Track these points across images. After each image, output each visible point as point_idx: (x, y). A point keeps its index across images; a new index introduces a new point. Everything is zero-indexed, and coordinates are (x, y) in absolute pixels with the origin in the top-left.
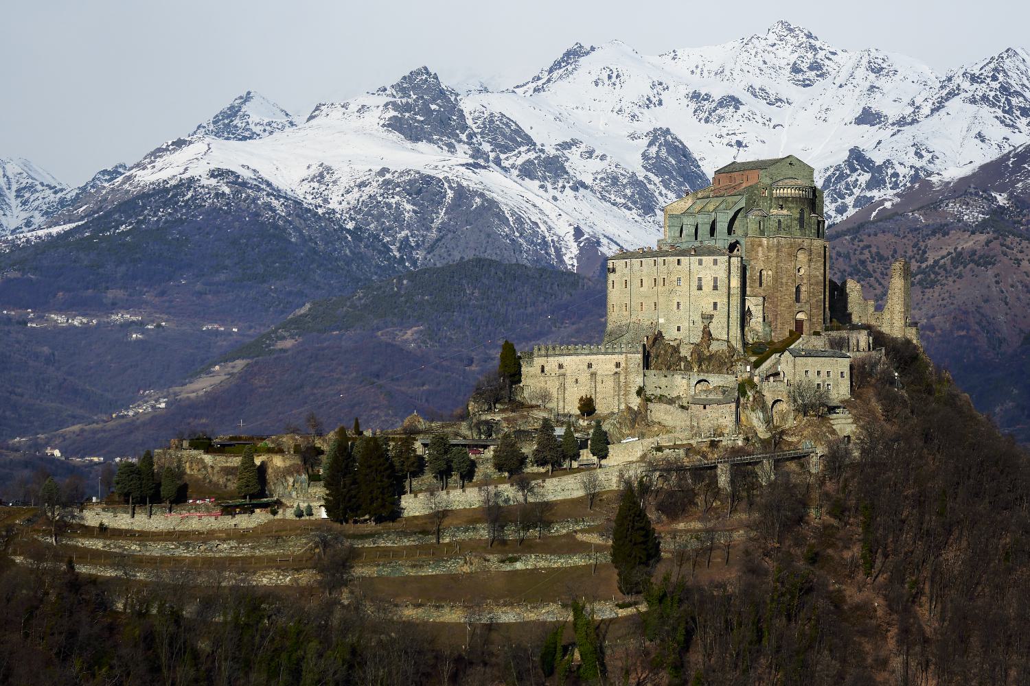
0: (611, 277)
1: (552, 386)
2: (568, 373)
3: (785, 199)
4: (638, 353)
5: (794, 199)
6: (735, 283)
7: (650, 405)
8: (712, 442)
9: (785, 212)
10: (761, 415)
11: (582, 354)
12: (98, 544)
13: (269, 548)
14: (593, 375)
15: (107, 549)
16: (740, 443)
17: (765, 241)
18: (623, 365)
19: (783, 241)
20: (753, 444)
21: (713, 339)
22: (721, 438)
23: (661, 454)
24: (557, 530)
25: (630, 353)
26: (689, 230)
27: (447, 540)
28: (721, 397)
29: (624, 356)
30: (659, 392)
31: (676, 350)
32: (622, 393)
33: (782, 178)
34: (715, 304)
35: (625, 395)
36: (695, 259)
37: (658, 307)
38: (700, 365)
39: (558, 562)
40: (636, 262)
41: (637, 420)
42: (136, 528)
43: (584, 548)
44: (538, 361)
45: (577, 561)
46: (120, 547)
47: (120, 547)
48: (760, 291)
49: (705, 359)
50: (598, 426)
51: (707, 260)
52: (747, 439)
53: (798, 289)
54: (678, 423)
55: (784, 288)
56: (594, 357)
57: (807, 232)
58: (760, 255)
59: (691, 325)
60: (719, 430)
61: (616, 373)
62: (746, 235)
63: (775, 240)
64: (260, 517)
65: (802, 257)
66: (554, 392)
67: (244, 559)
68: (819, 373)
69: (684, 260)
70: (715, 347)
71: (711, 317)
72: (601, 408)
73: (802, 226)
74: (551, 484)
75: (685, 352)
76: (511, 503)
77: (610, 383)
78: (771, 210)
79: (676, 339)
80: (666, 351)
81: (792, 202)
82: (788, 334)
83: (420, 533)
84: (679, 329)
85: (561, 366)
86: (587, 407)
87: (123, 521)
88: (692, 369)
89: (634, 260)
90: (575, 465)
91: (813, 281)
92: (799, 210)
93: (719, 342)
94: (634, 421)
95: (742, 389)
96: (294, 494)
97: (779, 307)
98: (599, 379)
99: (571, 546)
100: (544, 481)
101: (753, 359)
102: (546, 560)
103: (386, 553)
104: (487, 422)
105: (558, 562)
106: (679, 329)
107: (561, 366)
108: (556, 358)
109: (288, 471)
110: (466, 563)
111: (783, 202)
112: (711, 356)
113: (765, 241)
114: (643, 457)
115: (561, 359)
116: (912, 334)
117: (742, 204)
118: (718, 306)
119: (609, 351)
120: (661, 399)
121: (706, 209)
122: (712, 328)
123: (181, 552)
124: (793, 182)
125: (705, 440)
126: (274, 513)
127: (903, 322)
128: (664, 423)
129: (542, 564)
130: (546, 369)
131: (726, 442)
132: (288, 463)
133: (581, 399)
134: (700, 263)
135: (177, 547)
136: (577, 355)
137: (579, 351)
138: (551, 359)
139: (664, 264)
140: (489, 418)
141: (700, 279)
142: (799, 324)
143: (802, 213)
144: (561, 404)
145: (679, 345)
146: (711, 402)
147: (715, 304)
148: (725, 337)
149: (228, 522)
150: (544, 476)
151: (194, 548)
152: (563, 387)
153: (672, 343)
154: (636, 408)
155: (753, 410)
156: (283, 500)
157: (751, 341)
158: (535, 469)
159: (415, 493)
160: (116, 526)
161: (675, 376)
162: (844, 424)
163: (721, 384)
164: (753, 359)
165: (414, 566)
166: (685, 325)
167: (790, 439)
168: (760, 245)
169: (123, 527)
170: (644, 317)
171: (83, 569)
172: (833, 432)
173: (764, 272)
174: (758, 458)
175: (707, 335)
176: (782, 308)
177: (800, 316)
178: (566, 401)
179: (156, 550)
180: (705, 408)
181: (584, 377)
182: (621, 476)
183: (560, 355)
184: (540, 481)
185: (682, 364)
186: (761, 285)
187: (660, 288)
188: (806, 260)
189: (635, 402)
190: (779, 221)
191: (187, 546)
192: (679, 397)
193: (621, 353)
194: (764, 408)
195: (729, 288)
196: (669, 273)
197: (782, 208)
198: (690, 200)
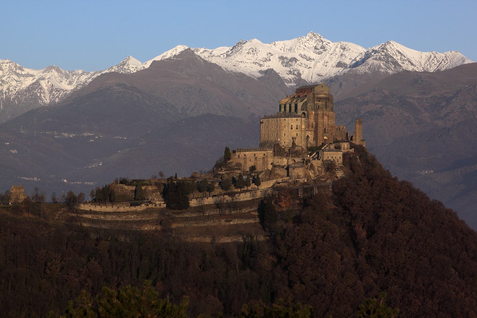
0: (262, 125)
1: (242, 162)
2: (248, 157)
6: (303, 127)
7: (275, 168)
9: (320, 103)
12: (89, 216)
13: (147, 217)
14: (256, 158)
15: (93, 218)
16: (306, 181)
19: (319, 112)
21: (296, 146)
22: (299, 179)
23: (279, 185)
24: (244, 211)
26: (288, 109)
27: (207, 214)
29: (266, 151)
31: (284, 149)
33: (319, 91)
34: (297, 134)
38: (292, 155)
39: (245, 222)
40: (270, 120)
41: (271, 174)
42: (102, 211)
43: (254, 217)
45: (252, 221)
46: (97, 217)
47: (97, 217)
48: (311, 129)
49: (293, 151)
50: (258, 176)
51: (294, 119)
52: (307, 180)
53: (325, 129)
56: (256, 152)
58: (312, 117)
61: (264, 157)
64: (143, 207)
65: (326, 118)
66: (243, 164)
67: (139, 221)
68: (332, 157)
70: (296, 149)
71: (296, 138)
72: (258, 169)
73: (326, 107)
74: (242, 195)
76: (229, 201)
77: (261, 161)
80: (280, 150)
81: (323, 99)
82: (321, 144)
83: (198, 212)
84: (285, 142)
85: (245, 155)
86: (253, 168)
87: (98, 208)
90: (250, 188)
93: (298, 147)
94: (270, 174)
96: (155, 199)
98: (258, 159)
99: (248, 216)
100: (240, 194)
101: (310, 152)
102: (241, 221)
103: (187, 219)
104: (220, 174)
105: (245, 222)
106: (285, 142)
108: (244, 153)
109: (153, 191)
110: (214, 222)
111: (320, 99)
112: (296, 151)
113: (313, 112)
115: (245, 153)
117: (306, 100)
118: (298, 134)
120: (279, 166)
123: (118, 219)
126: (148, 205)
127: (360, 139)
128: (280, 174)
129: (239, 222)
130: (240, 156)
131: (301, 181)
132: (153, 189)
135: (116, 217)
138: (241, 153)
140: (221, 173)
142: (326, 140)
143: (326, 103)
144: (245, 168)
145: (285, 148)
146: (296, 167)
147: (297, 134)
149: (133, 208)
150: (240, 193)
151: (122, 218)
152: (245, 162)
153: (283, 147)
154: (270, 169)
156: (152, 201)
157: (309, 146)
158: (236, 190)
159: (196, 198)
160: (96, 210)
162: (340, 174)
164: (310, 152)
165: (196, 223)
167: (322, 180)
168: (312, 114)
169: (98, 210)
170: (272, 139)
171: (85, 225)
172: (337, 177)
173: (313, 123)
175: (294, 144)
179: (109, 218)
180: (294, 169)
181: (253, 159)
183: (245, 151)
184: (239, 194)
185: (286, 154)
186: (312, 127)
189: (270, 167)
190: (319, 106)
191: (120, 217)
193: (265, 151)
197: (319, 101)
198: (288, 99)
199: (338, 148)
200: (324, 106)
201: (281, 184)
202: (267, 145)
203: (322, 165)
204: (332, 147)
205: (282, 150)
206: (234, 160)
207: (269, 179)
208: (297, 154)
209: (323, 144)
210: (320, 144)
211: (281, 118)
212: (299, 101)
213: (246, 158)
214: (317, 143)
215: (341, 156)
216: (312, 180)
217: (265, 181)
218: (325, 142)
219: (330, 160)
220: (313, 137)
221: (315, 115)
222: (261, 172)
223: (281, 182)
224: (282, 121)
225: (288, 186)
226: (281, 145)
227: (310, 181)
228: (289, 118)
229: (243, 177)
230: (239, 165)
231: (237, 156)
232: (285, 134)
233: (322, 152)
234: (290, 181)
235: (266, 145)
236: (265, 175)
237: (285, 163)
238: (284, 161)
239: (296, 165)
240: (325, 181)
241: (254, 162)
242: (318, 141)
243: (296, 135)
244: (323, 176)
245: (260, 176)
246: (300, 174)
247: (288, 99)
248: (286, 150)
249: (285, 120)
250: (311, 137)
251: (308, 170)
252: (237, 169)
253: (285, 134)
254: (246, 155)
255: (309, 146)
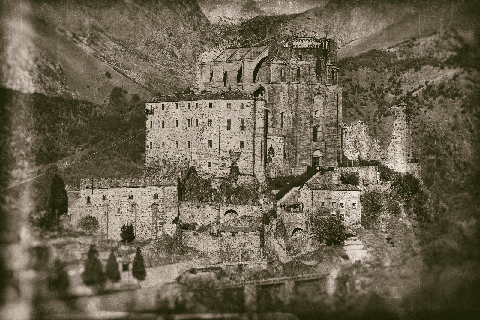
0: (150, 118)
2: (112, 203)
3: (304, 50)
4: (175, 186)
5: (312, 50)
6: (260, 124)
7: (185, 233)
8: (240, 266)
9: (303, 61)
10: (283, 242)
11: (123, 187)
14: (134, 205)
17: (286, 87)
18: (160, 197)
19: (302, 87)
20: (276, 268)
22: (247, 262)
23: (193, 276)
25: (167, 186)
28: (248, 226)
29: (161, 188)
30: (192, 221)
31: (207, 183)
32: (160, 221)
33: (301, 31)
34: (242, 143)
35: (162, 223)
36: (224, 103)
37: (193, 145)
38: (229, 197)
40: (172, 105)
41: (174, 247)
44: (84, 193)
49: (233, 191)
50: (139, 251)
51: (236, 103)
52: (270, 263)
54: (209, 248)
55: (303, 129)
56: (136, 189)
57: (323, 79)
58: (282, 99)
59: (221, 161)
60: (246, 256)
61: (154, 204)
62: (269, 81)
63: (295, 85)
66: (99, 219)
69: (215, 103)
70: (241, 181)
71: (238, 154)
72: (140, 235)
73: (318, 75)
75: (215, 185)
77: (149, 213)
78: (292, 60)
79: (207, 174)
80: (198, 185)
81: (310, 52)
82: (306, 169)
84: (210, 165)
85: (105, 198)
86: (128, 233)
88: (221, 201)
89: (170, 104)
90: (117, 286)
91: (328, 122)
92: (316, 59)
93: (246, 177)
94: (171, 246)
95: (266, 218)
97: (298, 146)
98: (139, 208)
101: (275, 192)
106: (210, 165)
107: (105, 198)
108: (101, 190)
111: (302, 52)
112: (239, 189)
113: (286, 87)
114: (179, 279)
115: (105, 191)
116: (414, 169)
117: (266, 54)
119: (149, 184)
121: (234, 58)
122: (239, 164)
124: (311, 35)
125: (234, 264)
128: (197, 248)
130: (91, 200)
131: (250, 265)
133: (123, 227)
134: (229, 106)
136: (120, 187)
137: (121, 184)
138: (96, 191)
139: (197, 107)
141: (229, 121)
142: (316, 160)
143: (318, 62)
145: (210, 179)
147: (242, 143)
148: (250, 172)
152: (106, 215)
153: (203, 177)
154: (172, 235)
155: (276, 238)
157: (273, 176)
161: (207, 206)
163: (247, 214)
164: (275, 192)
166: (215, 161)
167: (307, 263)
168: (282, 90)
172: (346, 257)
174: (282, 280)
175: (234, 169)
176: (301, 145)
177: (317, 154)
178: (110, 228)
180: (233, 235)
181: (125, 208)
182: (159, 296)
185: (213, 196)
186: (282, 126)
187: (194, 128)
188: (322, 103)
189: (171, 229)
190: (299, 69)
192: (209, 225)
193: (159, 186)
194: (285, 237)
195: (255, 129)
196: (202, 115)
197: (301, 58)
199: (350, 181)
200: (314, 70)
201: (199, 274)
202: (163, 172)
203: (307, 225)
204: (335, 178)
205: (202, 184)
206: (77, 210)
207: (168, 262)
208: (244, 195)
209: (311, 172)
210: (301, 170)
211: (201, 102)
212: (248, 56)
213: (107, 205)
214: (294, 166)
215: (357, 201)
216: (282, 264)
217: (157, 264)
218: (314, 163)
219: (327, 212)
220: (283, 153)
221: (290, 94)
222: (145, 243)
223: (199, 270)
224: (203, 109)
225: (219, 278)
226: (199, 171)
227: (276, 268)
228: (221, 99)
229: (98, 254)
230: (90, 223)
231: (83, 200)
232: (210, 143)
233: (309, 191)
234: (221, 265)
235: (160, 170)
236: (156, 251)
237: (212, 219)
238: (208, 214)
239: (239, 225)
240: (316, 266)
241: (129, 217)
242: (298, 162)
243: (239, 145)
244: (309, 253)
245: (145, 251)
246: (248, 247)
247: (219, 51)
248: (212, 184)
249: (211, 105)
250: (279, 150)
251: (271, 239)
252: (82, 234)
253: (210, 143)
254: (108, 196)
255: (273, 173)
